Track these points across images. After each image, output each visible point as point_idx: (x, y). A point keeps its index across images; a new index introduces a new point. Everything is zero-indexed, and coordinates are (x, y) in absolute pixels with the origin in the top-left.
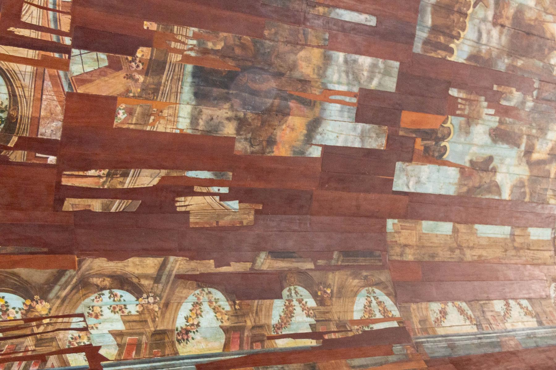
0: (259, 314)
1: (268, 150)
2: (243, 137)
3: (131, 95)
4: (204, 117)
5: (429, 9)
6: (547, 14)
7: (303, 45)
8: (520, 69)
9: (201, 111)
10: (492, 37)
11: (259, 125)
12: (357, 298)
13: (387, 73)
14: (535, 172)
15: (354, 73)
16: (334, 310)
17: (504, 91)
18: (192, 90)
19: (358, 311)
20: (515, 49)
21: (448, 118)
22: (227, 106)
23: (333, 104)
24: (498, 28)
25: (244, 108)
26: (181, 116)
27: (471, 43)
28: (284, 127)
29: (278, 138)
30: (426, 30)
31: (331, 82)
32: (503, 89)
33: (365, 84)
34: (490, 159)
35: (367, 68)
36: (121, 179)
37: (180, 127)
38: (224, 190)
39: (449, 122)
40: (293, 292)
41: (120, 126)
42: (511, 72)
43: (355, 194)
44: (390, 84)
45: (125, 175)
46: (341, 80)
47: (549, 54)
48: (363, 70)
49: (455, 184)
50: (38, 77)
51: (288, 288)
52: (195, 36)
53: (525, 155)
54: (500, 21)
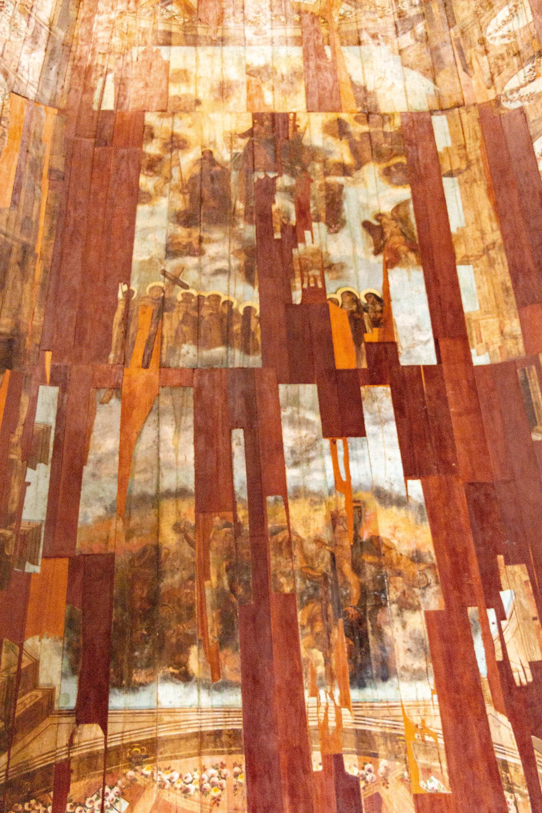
1: (429, 560)
2: (421, 599)
3: (406, 774)
5: (205, 353)
6: (171, 177)
7: (290, 532)
8: (247, 203)
10: (217, 253)
11: (400, 579)
13: (295, 401)
14: (367, 154)
15: (307, 451)
17: (278, 221)
18: (380, 684)
20: (223, 215)
21: (331, 299)
22: (387, 630)
23: (352, 474)
24: (205, 246)
25: (386, 606)
27: (232, 282)
28: (395, 542)
30: (231, 353)
31: (326, 482)
32: (276, 223)
33: (316, 431)
34: (366, 225)
35: (297, 431)
36: (512, 770)
39: (334, 296)
41: (448, 784)
42: (254, 217)
43: (454, 419)
44: (309, 392)
45: (505, 764)
46: (320, 467)
47: (218, 164)
48: (301, 437)
49: (408, 271)
52: (314, 694)
53: (349, 175)
54: (195, 245)
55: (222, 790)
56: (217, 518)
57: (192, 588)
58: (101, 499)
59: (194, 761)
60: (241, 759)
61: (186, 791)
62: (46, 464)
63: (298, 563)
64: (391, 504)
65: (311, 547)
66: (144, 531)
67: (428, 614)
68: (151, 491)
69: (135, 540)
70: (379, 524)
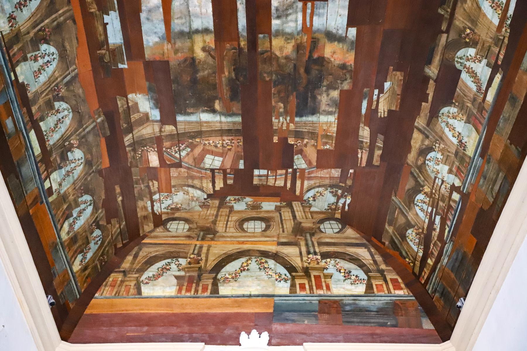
0: (466, 94)
2: (340, 85)
4: (327, 109)
7: (271, 53)
9: (324, 111)
12: (482, 8)
15: (287, 9)
16: (484, 38)
19: (492, 18)
23: (314, 23)
25: (320, 87)
26: (327, 121)
28: (332, 59)
29: (341, 63)
36: (364, 144)
37: (334, 120)
38: (376, 92)
40: (459, 60)
46: (294, 19)
50: (309, 179)
51: (456, 63)
52: (278, 118)
55: (232, 146)
56: (228, 45)
57: (215, 77)
58: (155, 33)
59: (220, 138)
60: (241, 138)
61: (216, 146)
62: (115, 11)
63: (274, 68)
64: (335, 41)
65: (283, 61)
66: (185, 51)
67: (342, 92)
68: (186, 30)
69: (179, 55)
70: (325, 50)
